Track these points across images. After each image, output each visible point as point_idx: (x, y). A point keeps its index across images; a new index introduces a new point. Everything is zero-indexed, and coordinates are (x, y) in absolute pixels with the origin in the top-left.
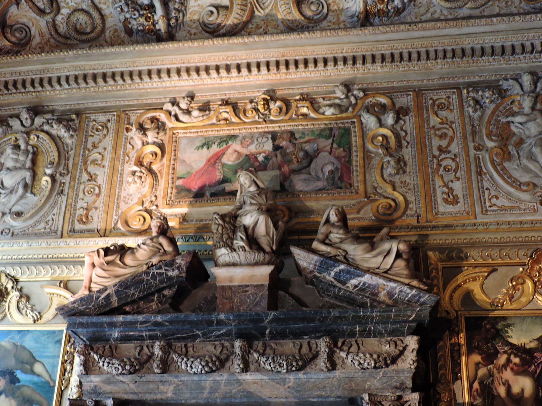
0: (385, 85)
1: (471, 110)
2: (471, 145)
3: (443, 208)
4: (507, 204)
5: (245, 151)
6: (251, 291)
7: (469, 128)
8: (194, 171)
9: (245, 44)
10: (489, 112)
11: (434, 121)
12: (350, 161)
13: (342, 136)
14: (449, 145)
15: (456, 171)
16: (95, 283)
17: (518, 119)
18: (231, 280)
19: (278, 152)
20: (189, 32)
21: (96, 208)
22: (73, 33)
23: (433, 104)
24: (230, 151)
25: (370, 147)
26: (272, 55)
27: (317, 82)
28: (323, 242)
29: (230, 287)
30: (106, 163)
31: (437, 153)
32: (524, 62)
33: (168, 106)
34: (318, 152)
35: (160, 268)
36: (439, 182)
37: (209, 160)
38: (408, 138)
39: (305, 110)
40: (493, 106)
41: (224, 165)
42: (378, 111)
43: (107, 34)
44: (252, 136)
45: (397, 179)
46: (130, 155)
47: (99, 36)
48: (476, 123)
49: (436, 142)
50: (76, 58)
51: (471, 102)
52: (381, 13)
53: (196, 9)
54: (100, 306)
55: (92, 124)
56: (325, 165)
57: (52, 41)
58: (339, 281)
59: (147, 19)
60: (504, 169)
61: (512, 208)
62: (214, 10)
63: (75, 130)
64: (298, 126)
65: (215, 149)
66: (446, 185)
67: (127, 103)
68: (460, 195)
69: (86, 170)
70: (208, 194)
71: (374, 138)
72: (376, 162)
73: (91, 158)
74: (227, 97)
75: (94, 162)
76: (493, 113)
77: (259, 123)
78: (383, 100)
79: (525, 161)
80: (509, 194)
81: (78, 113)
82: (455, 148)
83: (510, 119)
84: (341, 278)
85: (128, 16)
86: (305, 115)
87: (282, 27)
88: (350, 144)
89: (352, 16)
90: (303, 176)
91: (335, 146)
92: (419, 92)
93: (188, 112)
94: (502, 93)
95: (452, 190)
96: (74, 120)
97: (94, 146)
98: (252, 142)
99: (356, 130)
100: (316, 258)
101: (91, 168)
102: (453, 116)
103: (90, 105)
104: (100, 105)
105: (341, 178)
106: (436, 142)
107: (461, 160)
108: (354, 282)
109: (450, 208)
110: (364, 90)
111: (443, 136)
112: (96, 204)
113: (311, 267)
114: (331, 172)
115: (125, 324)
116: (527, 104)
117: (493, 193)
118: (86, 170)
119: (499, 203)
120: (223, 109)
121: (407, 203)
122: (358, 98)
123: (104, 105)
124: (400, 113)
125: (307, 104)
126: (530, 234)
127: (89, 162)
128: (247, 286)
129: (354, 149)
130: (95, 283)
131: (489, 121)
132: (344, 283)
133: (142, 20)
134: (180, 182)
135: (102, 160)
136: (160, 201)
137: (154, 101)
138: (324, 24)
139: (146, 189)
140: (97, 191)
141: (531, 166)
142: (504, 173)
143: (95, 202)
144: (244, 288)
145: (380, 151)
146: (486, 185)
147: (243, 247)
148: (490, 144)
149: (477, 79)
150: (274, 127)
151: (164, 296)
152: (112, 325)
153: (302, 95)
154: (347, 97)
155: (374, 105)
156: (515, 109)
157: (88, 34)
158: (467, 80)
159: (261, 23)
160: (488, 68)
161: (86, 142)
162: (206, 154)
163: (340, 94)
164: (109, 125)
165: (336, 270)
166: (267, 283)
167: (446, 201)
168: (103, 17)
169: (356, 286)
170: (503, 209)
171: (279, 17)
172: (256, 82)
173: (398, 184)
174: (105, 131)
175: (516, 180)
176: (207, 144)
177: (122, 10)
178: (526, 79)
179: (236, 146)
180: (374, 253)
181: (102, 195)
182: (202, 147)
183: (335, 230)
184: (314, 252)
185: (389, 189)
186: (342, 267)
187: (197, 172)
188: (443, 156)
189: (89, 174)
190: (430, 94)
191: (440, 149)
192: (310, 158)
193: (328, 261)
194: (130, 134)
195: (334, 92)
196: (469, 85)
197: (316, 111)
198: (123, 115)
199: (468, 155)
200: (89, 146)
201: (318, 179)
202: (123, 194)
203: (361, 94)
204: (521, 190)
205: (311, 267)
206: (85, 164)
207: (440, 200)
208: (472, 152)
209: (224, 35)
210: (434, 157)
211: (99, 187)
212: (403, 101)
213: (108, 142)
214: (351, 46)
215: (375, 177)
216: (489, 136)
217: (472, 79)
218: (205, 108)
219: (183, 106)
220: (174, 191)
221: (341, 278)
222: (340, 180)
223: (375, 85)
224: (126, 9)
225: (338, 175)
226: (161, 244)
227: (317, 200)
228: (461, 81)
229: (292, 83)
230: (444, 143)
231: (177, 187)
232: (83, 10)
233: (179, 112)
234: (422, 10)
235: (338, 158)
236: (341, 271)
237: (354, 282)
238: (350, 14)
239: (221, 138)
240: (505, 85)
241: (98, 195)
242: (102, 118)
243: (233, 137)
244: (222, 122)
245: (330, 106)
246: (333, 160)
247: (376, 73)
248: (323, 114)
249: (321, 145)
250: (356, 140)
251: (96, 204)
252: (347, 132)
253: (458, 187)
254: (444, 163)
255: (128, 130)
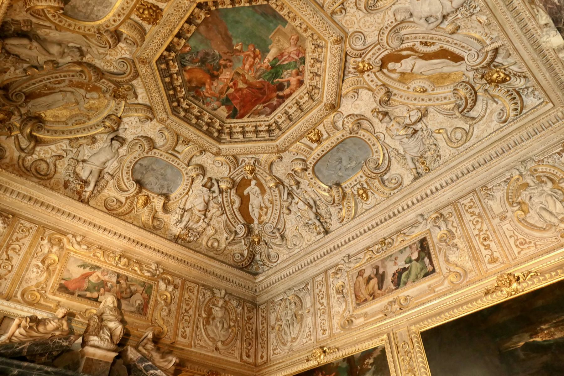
0: (172, 271)
1: (201, 297)
2: (197, 313)
3: (180, 339)
4: (204, 345)
5: (102, 278)
6: (102, 364)
7: (198, 305)
8: (72, 278)
9: (125, 226)
10: (207, 300)
11: (186, 296)
12: (148, 302)
13: (149, 288)
14: (189, 309)
15: (189, 323)
16: (15, 337)
17: (217, 309)
18: (94, 355)
19: (118, 285)
20: (97, 203)
21: (6, 279)
22: (33, 170)
23: (188, 288)
24: (95, 274)
25: (159, 299)
26: (133, 236)
27: (145, 256)
28: (144, 347)
29: (92, 359)
30: (22, 253)
31: (184, 312)
32: (223, 284)
33: (70, 236)
34: (136, 292)
35: (60, 339)
36: (181, 326)
37: (82, 275)
38: (175, 300)
39: (136, 268)
40: (209, 298)
41: (89, 281)
42: (169, 283)
43: (53, 181)
44: (108, 271)
45: (166, 318)
46: (39, 254)
47: (48, 179)
48: (201, 303)
49: (185, 307)
50: (33, 187)
51: (203, 294)
52: (183, 239)
53: (106, 194)
54: (15, 353)
55: (20, 225)
56: (138, 300)
57: (17, 166)
58: (145, 370)
59: (81, 187)
60: (206, 328)
61: (205, 347)
62: (115, 201)
63: (8, 225)
64: (131, 275)
65: (87, 270)
66: (183, 328)
67: (46, 223)
68: (188, 335)
69: (7, 253)
70: (77, 294)
71: (161, 295)
72: (159, 307)
73: (12, 246)
74: (102, 245)
75: (14, 249)
76: (208, 302)
77: (114, 266)
78: (170, 278)
79: (214, 328)
80: (205, 340)
81: (14, 215)
82: (191, 312)
83: (214, 307)
84: (147, 369)
85: (71, 180)
86: (136, 271)
87: (141, 224)
88: (151, 293)
89: (171, 234)
90: (126, 302)
91: (144, 292)
92: (184, 280)
93: (79, 243)
94: (213, 293)
95: (185, 331)
96: (9, 218)
97: (17, 240)
98: (107, 275)
99: (154, 287)
100: (140, 355)
101: (10, 252)
102: (194, 297)
103: (23, 214)
104: (29, 216)
105: (143, 309)
106: (185, 307)
107: (192, 318)
108: (152, 372)
109: (182, 340)
110: (164, 270)
111: (188, 305)
112: (7, 277)
113: (135, 359)
114: (139, 305)
115: (26, 367)
116: (221, 303)
117: (200, 338)
118: (7, 253)
119: (202, 343)
120: (98, 251)
121: (167, 332)
122: (163, 274)
123: (32, 217)
124: (176, 287)
125: (138, 266)
126: (210, 362)
127: (10, 248)
128: (101, 361)
129: (152, 297)
130: (15, 337)
131: (206, 305)
132: (147, 371)
133: (78, 187)
134: (63, 282)
135: (19, 250)
136: (49, 289)
137: (62, 229)
138: (158, 232)
139: (42, 279)
140: (10, 268)
141: (215, 330)
142: (206, 330)
143: (6, 275)
144: (99, 361)
145: (163, 302)
146: (198, 333)
147: (108, 340)
148: (204, 315)
149: (206, 284)
150: (120, 271)
151: (52, 354)
152: (19, 367)
153: (137, 260)
154: (156, 270)
155: (165, 279)
156: (216, 303)
157: (41, 175)
158: (202, 282)
159: (132, 217)
160: (211, 280)
161: (12, 235)
162: (82, 271)
163: (153, 267)
164: (31, 231)
165: (146, 364)
166: (111, 362)
167: (182, 335)
168: (55, 172)
169: (151, 374)
170: (202, 346)
171: (143, 219)
172: (119, 244)
173: (165, 321)
174: (27, 234)
175: (209, 335)
176: (84, 266)
177: (70, 176)
178: (223, 292)
179: (98, 273)
180: (164, 360)
181: (13, 272)
182: (81, 266)
183: (150, 343)
184: (139, 351)
185: (162, 323)
186: (150, 363)
187: (76, 279)
188: (186, 314)
189: (8, 255)
190: (188, 283)
191: (185, 310)
192: (132, 294)
193: (144, 359)
194: (42, 242)
195: (151, 265)
196: (203, 285)
197: (141, 271)
198: (41, 229)
199: (195, 317)
200: (14, 238)
201: (133, 306)
202: (26, 276)
203: (162, 271)
204: (209, 340)
205: (135, 359)
206: (7, 248)
207: (180, 335)
208: (197, 316)
209: (113, 215)
210: (182, 313)
211: (12, 266)
212: (178, 282)
213: (27, 241)
214: (168, 249)
215: (157, 315)
216: (205, 311)
217: (204, 283)
218: (89, 245)
219: (79, 239)
220: (58, 286)
221: (147, 369)
222: (142, 310)
223: (168, 269)
224: (72, 176)
225: (141, 307)
226: (62, 324)
227: (130, 317)
228: (200, 282)
229: (135, 252)
230: (188, 308)
231: (60, 284)
232: (46, 162)
233: (74, 241)
234: (198, 245)
235: (144, 298)
236: (148, 365)
237: (152, 372)
238: (171, 232)
239: (92, 265)
240: (215, 291)
241: (10, 271)
242: (28, 225)
243: (98, 268)
244: (95, 257)
245: (149, 271)
246: (142, 299)
247: (171, 264)
248: (143, 273)
249: (139, 289)
250: (154, 293)
251: (7, 277)
252: (151, 287)
253: (188, 330)
254: (185, 318)
255: (42, 239)
